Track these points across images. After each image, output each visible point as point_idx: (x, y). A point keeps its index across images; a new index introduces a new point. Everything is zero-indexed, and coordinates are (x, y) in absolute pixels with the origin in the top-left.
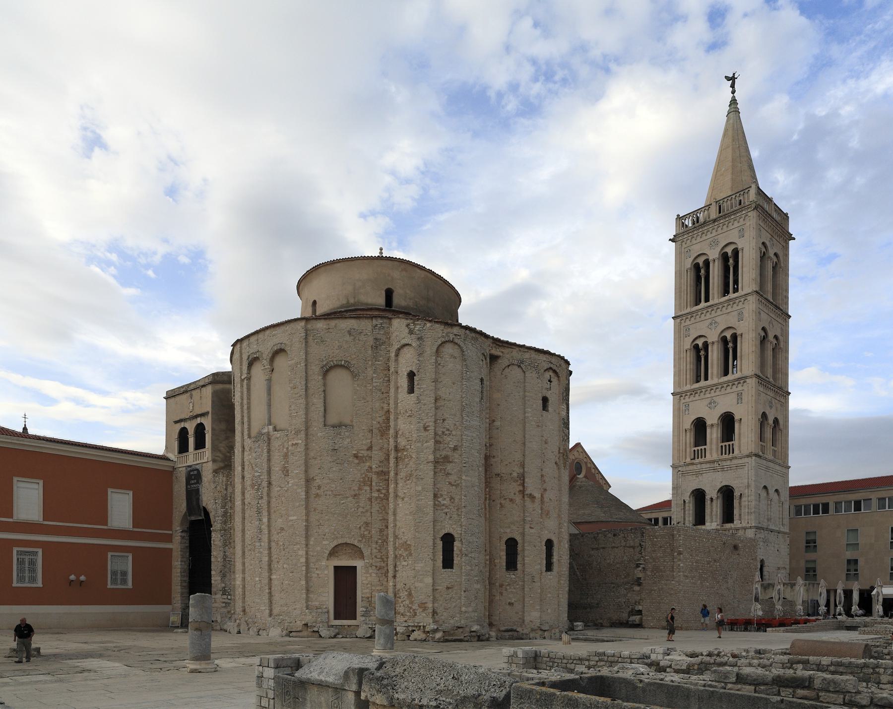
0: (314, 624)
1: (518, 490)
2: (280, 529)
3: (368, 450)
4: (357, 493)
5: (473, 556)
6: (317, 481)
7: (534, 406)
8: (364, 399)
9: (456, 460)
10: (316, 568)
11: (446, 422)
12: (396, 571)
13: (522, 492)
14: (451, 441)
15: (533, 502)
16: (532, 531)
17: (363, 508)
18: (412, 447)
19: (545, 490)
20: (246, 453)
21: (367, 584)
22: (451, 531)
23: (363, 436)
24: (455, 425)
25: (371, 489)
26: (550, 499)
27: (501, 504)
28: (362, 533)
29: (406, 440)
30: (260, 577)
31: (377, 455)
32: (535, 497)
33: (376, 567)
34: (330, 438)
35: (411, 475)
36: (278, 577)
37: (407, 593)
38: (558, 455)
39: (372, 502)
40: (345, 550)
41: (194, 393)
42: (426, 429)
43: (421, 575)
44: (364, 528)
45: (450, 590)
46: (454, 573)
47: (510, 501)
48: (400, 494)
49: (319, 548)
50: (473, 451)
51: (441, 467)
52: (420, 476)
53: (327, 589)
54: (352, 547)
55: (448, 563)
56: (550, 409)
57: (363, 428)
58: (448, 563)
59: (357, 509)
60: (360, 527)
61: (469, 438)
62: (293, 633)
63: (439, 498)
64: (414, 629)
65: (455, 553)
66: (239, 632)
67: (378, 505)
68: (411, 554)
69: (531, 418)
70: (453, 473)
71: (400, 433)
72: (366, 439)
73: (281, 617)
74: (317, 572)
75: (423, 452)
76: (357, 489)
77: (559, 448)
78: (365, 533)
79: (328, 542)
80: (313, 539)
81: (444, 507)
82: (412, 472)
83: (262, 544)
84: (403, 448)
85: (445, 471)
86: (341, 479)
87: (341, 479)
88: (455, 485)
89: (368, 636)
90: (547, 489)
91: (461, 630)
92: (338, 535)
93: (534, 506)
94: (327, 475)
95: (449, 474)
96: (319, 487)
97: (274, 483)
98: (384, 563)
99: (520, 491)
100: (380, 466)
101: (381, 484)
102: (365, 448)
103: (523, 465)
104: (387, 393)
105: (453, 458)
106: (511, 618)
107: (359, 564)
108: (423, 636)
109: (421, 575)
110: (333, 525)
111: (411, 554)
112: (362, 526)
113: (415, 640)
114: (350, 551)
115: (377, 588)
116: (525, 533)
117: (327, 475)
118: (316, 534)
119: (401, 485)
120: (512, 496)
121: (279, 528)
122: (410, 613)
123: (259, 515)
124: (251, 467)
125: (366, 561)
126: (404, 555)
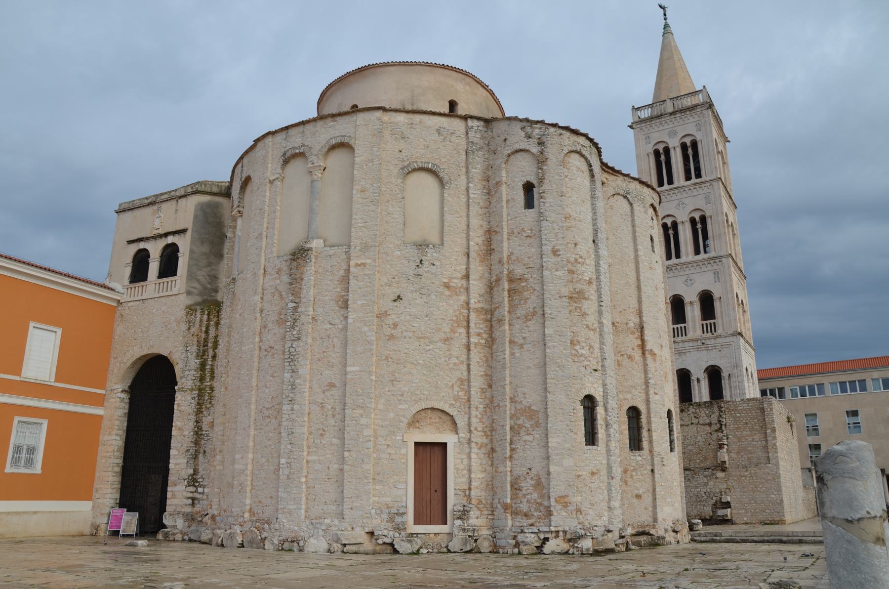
0: (385, 532)
1: (636, 344)
2: (327, 386)
3: (462, 278)
4: (449, 336)
6: (393, 317)
8: (457, 212)
9: (591, 297)
10: (388, 445)
11: (578, 247)
12: (512, 450)
13: (643, 346)
14: (588, 272)
15: (655, 360)
16: (657, 397)
17: (457, 358)
18: (534, 276)
20: (268, 277)
21: (462, 470)
22: (592, 392)
23: (456, 260)
24: (588, 252)
25: (468, 333)
29: (524, 267)
30: (289, 458)
31: (477, 287)
32: (655, 354)
33: (477, 443)
34: (411, 259)
36: (322, 458)
37: (533, 482)
39: (469, 350)
40: (430, 418)
41: (165, 206)
42: (555, 253)
43: (557, 454)
44: (459, 387)
45: (596, 477)
46: (599, 452)
47: (629, 358)
48: (516, 340)
49: (392, 415)
51: (576, 305)
52: (551, 314)
53: (405, 477)
54: (440, 414)
55: (591, 438)
56: (655, 250)
58: (591, 438)
59: (449, 358)
60: (453, 386)
62: (348, 547)
63: (574, 345)
64: (547, 536)
66: (242, 545)
67: (477, 354)
69: (643, 258)
71: (513, 258)
72: (460, 264)
73: (327, 521)
74: (389, 451)
75: (553, 283)
76: (449, 330)
78: (460, 394)
79: (407, 406)
80: (382, 401)
81: (582, 359)
82: (536, 309)
83: (296, 407)
84: (519, 277)
85: (580, 309)
86: (427, 316)
87: (427, 316)
88: (593, 330)
89: (468, 548)
91: (610, 535)
92: (422, 396)
94: (408, 310)
95: (584, 315)
96: (395, 326)
97: (321, 318)
98: (487, 438)
99: (639, 346)
100: (479, 301)
101: (481, 326)
102: (459, 275)
103: (640, 314)
104: (487, 208)
106: (639, 516)
107: (450, 439)
108: (565, 546)
109: (557, 454)
110: (415, 381)
111: (540, 424)
112: (456, 383)
113: (553, 553)
114: (437, 420)
115: (478, 476)
116: (650, 400)
117: (408, 310)
118: (389, 393)
119: (517, 326)
120: (629, 351)
121: (327, 384)
122: (540, 511)
123: (292, 364)
124: (277, 297)
125: (461, 435)
126: (528, 425)
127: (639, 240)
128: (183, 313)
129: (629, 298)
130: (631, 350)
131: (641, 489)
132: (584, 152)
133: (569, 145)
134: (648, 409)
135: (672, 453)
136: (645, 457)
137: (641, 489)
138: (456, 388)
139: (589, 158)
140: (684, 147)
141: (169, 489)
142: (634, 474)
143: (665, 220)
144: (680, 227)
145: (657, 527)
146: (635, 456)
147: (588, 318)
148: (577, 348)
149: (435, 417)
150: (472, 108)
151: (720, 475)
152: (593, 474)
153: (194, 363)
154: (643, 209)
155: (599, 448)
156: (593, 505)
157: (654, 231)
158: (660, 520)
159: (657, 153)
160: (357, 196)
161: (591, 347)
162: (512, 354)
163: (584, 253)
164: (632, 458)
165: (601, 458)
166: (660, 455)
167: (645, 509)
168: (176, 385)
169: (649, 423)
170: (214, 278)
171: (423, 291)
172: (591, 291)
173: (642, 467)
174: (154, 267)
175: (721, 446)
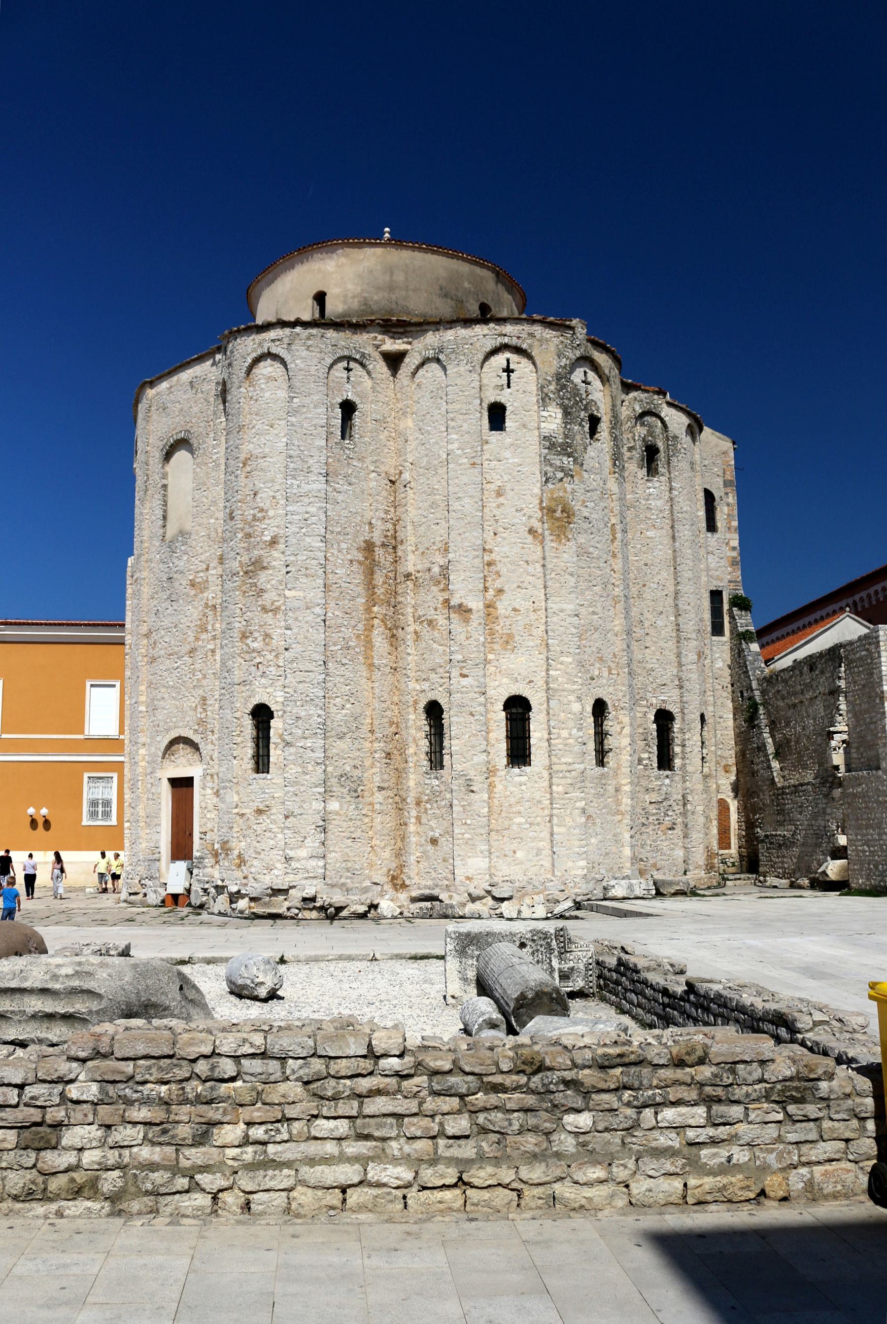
1: (441, 599)
5: (309, 745)
7: (465, 426)
9: (274, 563)
11: (259, 496)
16: (465, 682)
19: (500, 591)
22: (265, 700)
26: (515, 610)
27: (416, 632)
28: (199, 716)
32: (471, 610)
38: (539, 514)
47: (429, 625)
50: (308, 539)
55: (261, 763)
57: (203, 534)
58: (261, 763)
60: (196, 706)
61: (297, 517)
65: (271, 741)
70: (269, 586)
77: (542, 501)
81: (254, 655)
85: (256, 586)
86: (175, 627)
87: (175, 627)
90: (506, 589)
92: (171, 724)
93: (469, 628)
105: (269, 559)
107: (195, 771)
120: (431, 614)
129: (434, 527)
130: (433, 612)
131: (437, 830)
132: (274, 350)
133: (254, 350)
134: (450, 702)
135: (516, 770)
136: (443, 779)
137: (437, 830)
138: (199, 710)
139: (283, 353)
142: (428, 806)
145: (452, 888)
146: (430, 778)
147: (265, 596)
148: (249, 641)
150: (350, 286)
151: (837, 792)
152: (259, 812)
154: (469, 367)
155: (269, 776)
156: (259, 853)
157: (509, 390)
158: (460, 878)
161: (267, 636)
164: (427, 781)
165: (272, 790)
166: (465, 775)
167: (444, 861)
171: (174, 597)
172: (276, 558)
173: (438, 796)
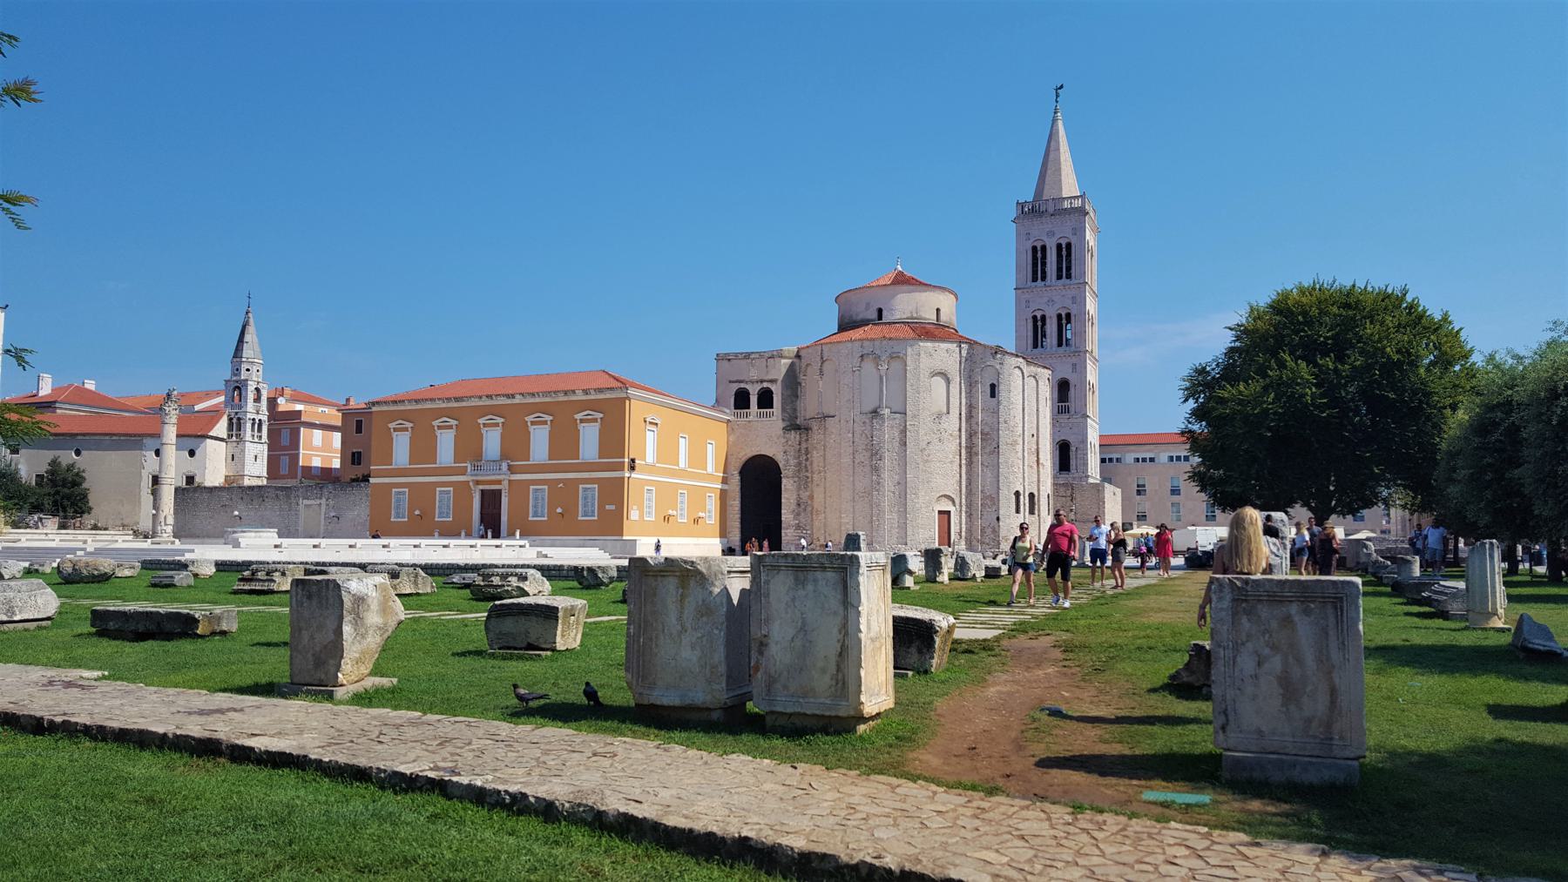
35: (994, 451)
42: (1006, 422)
68: (994, 504)
124: (864, 435)
127: (1040, 402)
128: (782, 432)
140: (1059, 247)
141: (783, 531)
143: (1034, 314)
144: (1048, 321)
149: (943, 499)
153: (793, 462)
159: (1034, 249)
160: (909, 388)
162: (982, 470)
163: (1018, 422)
168: (781, 473)
169: (1039, 501)
170: (795, 410)
174: (754, 400)
175: (1071, 510)
